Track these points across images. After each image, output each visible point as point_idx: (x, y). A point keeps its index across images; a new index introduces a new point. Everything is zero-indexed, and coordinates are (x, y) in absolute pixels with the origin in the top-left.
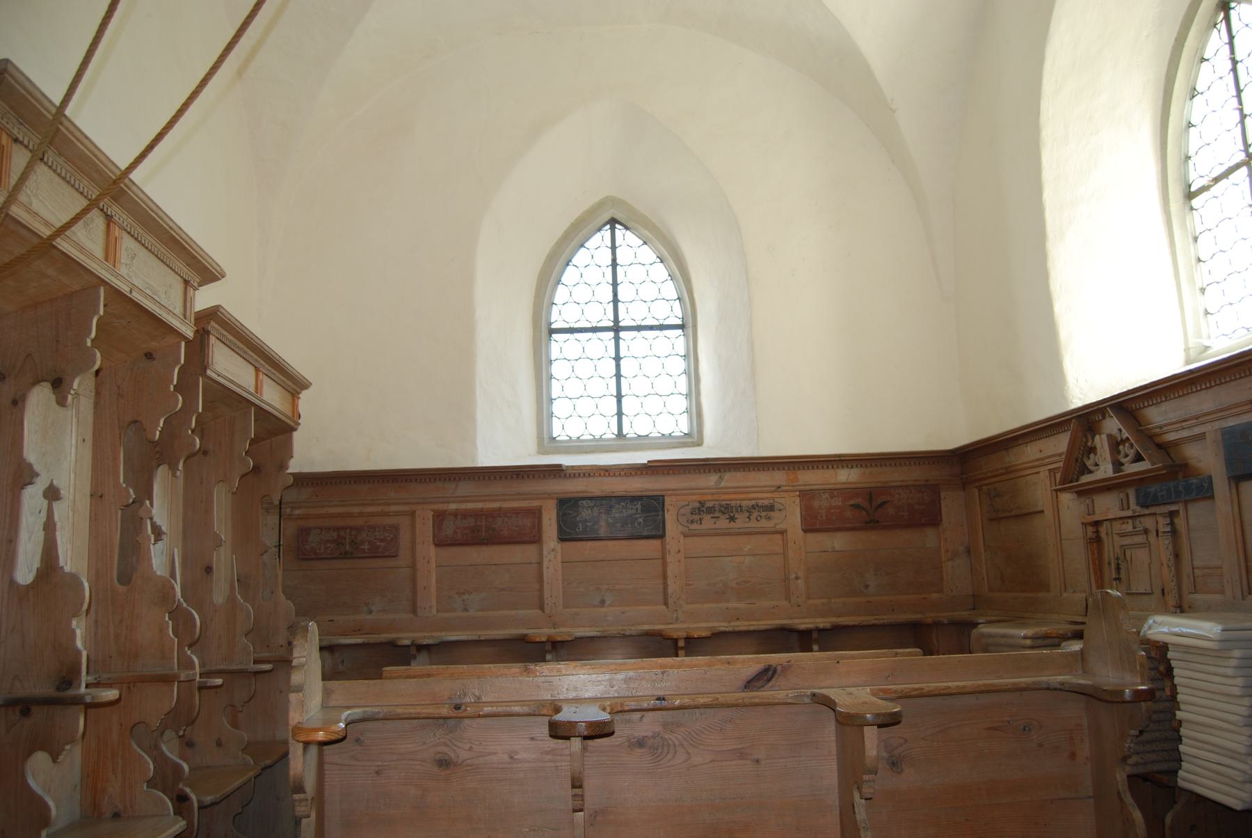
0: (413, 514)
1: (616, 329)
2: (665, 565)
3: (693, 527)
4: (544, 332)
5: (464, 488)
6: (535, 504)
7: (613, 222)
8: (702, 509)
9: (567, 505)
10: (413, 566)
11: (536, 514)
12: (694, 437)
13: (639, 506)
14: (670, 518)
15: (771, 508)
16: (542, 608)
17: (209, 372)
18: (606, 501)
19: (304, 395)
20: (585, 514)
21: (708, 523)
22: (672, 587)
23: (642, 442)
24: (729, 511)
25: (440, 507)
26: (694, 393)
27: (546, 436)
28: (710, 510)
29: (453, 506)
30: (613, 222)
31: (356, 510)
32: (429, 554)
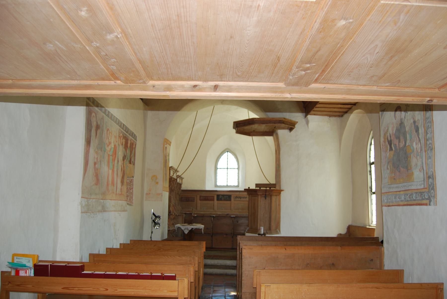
0: (197, 196)
1: (227, 168)
2: (231, 205)
3: (235, 200)
4: (216, 168)
5: (204, 193)
6: (213, 195)
7: (228, 152)
8: (236, 197)
9: (218, 196)
10: (197, 203)
11: (213, 197)
12: (238, 186)
13: (228, 196)
14: (232, 198)
15: (246, 198)
16: (214, 210)
17: (177, 182)
18: (223, 196)
19: (183, 180)
20: (220, 197)
21: (237, 199)
22: (232, 208)
23: (230, 186)
24: (240, 198)
25: (200, 195)
26: (238, 179)
27: (216, 185)
28: (238, 197)
29: (202, 195)
30: (228, 152)
31: (189, 195)
32: (199, 201)
